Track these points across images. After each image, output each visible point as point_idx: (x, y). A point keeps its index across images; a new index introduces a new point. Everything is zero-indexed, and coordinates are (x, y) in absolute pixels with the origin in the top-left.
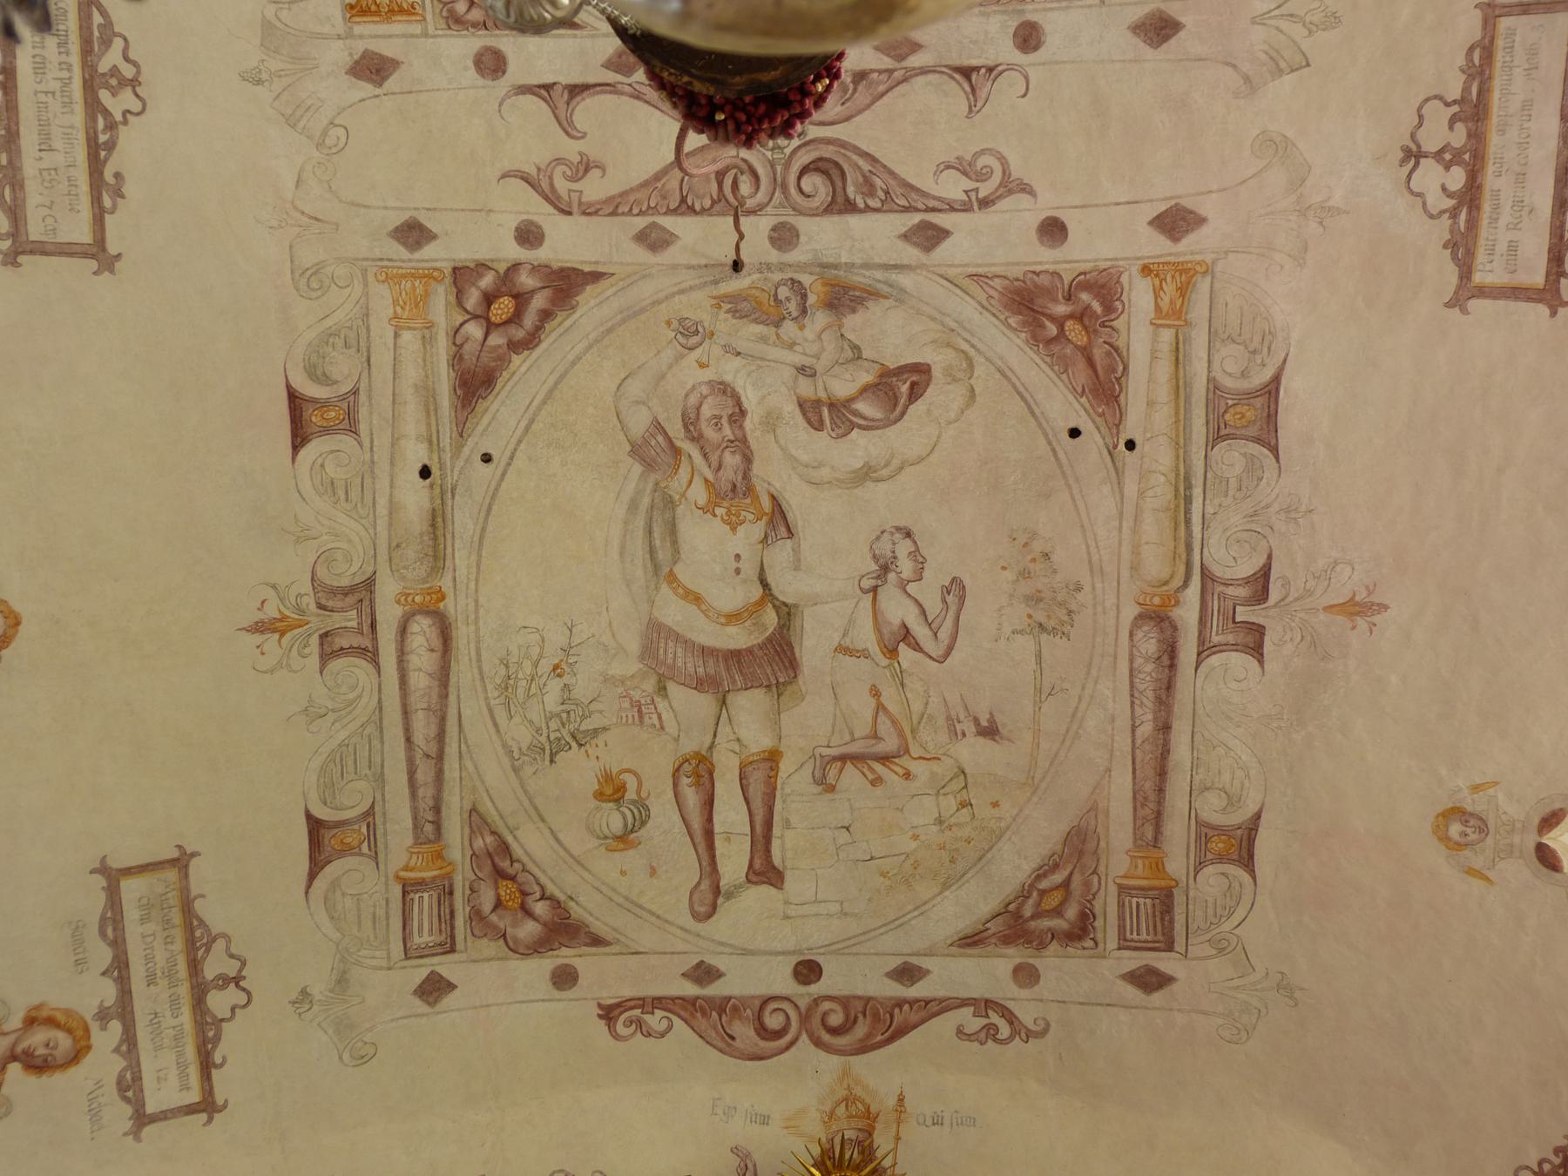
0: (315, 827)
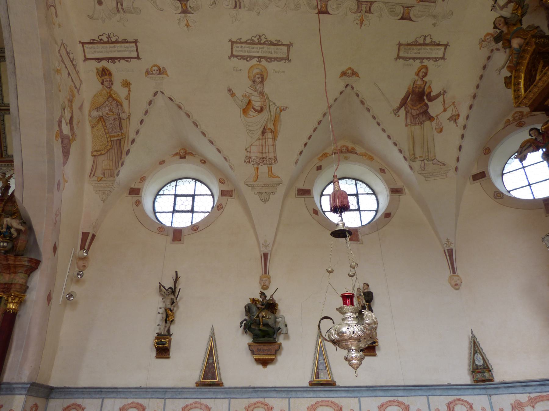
0: (402, 18)
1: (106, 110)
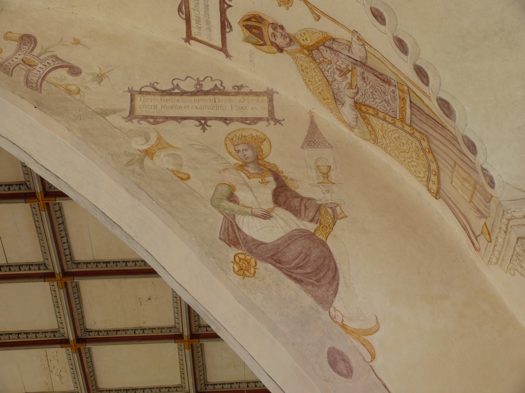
1: (341, 83)
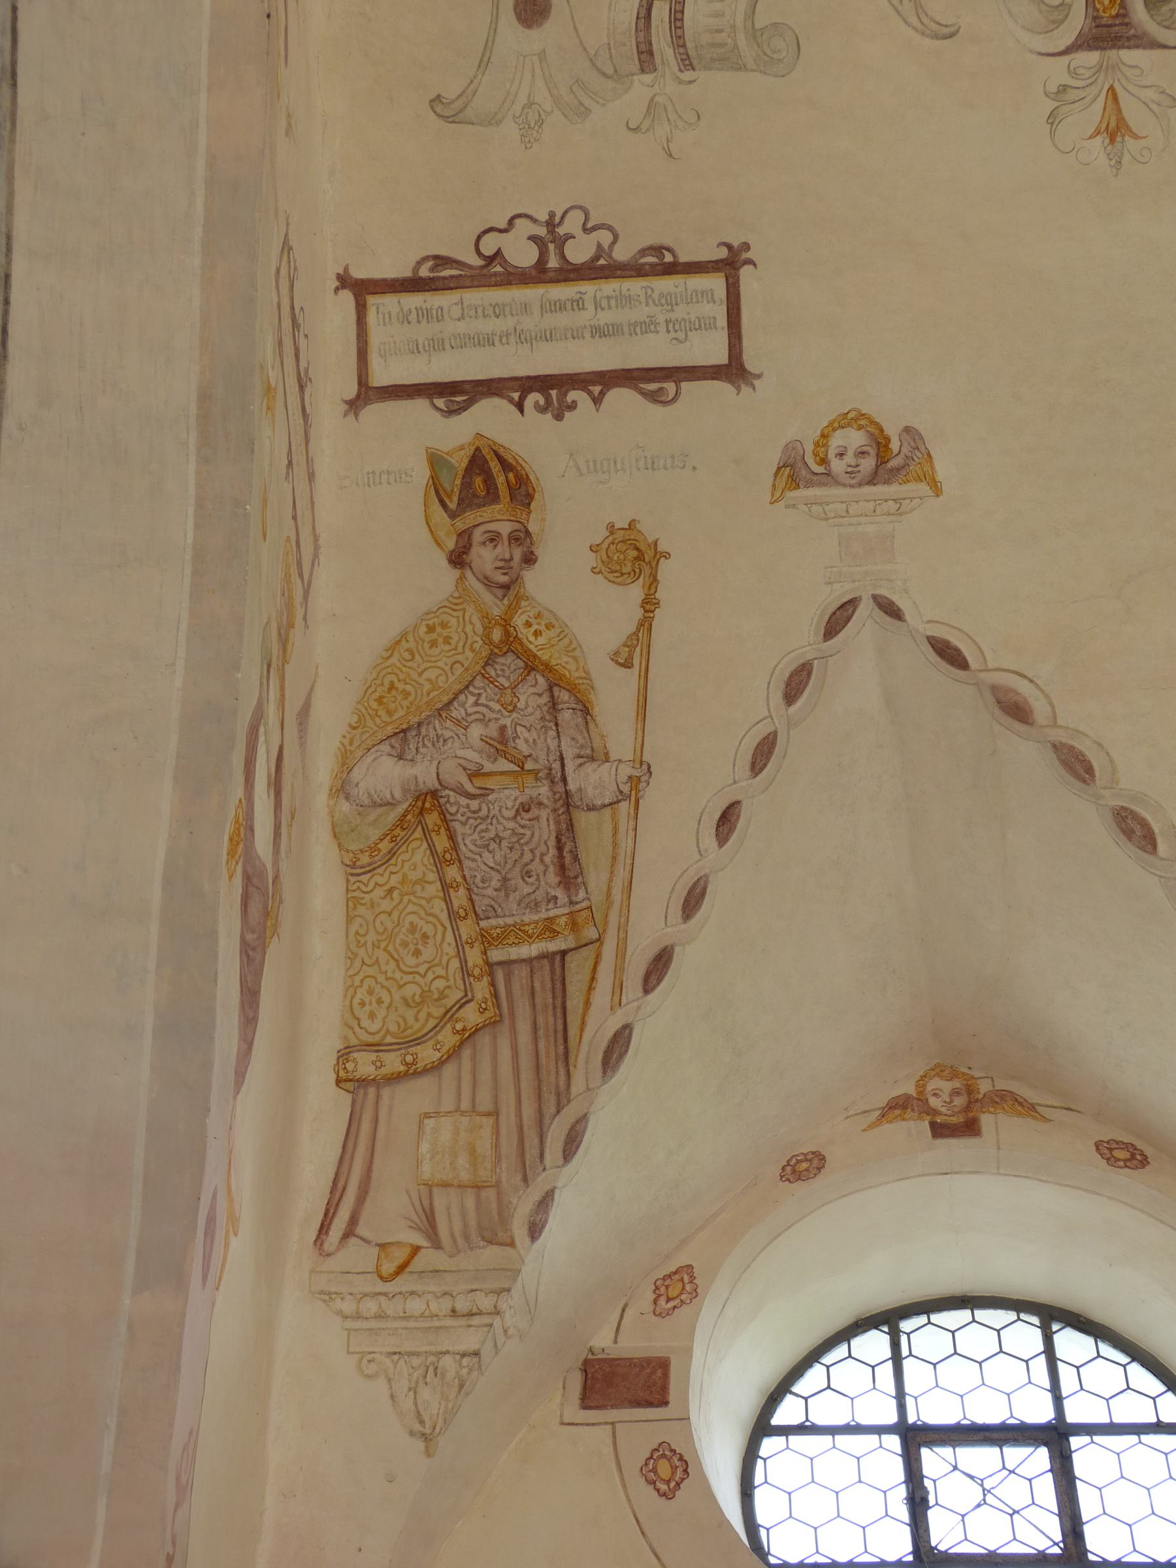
1: (465, 747)
